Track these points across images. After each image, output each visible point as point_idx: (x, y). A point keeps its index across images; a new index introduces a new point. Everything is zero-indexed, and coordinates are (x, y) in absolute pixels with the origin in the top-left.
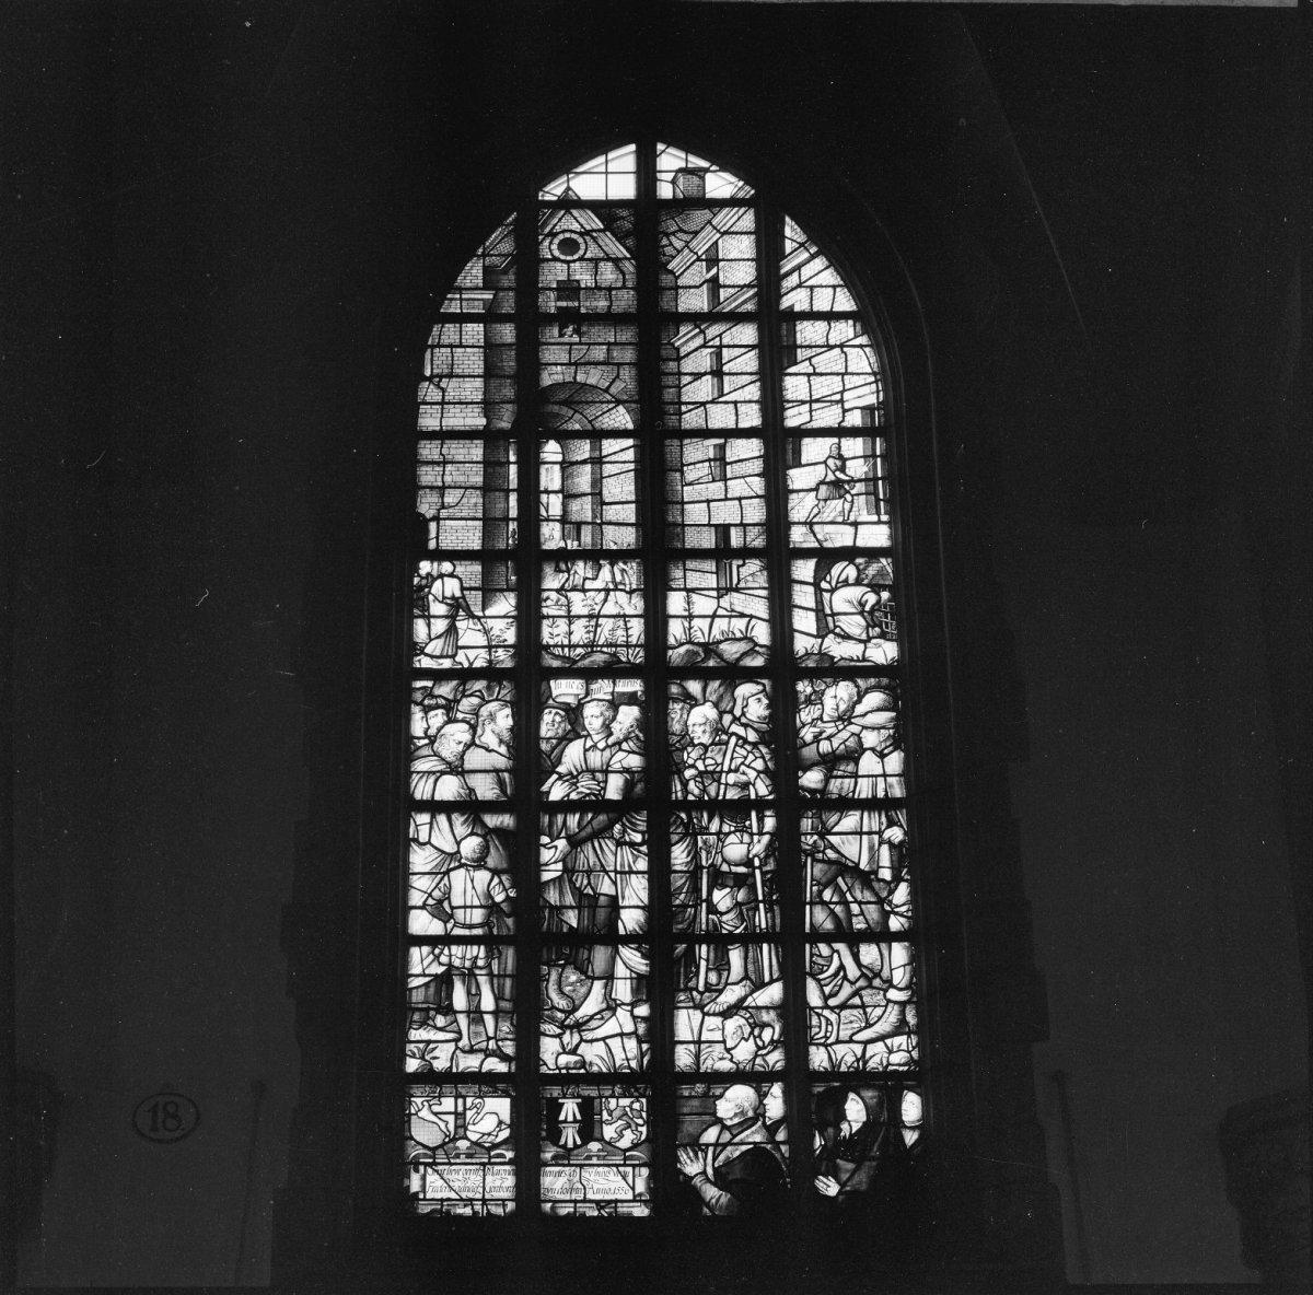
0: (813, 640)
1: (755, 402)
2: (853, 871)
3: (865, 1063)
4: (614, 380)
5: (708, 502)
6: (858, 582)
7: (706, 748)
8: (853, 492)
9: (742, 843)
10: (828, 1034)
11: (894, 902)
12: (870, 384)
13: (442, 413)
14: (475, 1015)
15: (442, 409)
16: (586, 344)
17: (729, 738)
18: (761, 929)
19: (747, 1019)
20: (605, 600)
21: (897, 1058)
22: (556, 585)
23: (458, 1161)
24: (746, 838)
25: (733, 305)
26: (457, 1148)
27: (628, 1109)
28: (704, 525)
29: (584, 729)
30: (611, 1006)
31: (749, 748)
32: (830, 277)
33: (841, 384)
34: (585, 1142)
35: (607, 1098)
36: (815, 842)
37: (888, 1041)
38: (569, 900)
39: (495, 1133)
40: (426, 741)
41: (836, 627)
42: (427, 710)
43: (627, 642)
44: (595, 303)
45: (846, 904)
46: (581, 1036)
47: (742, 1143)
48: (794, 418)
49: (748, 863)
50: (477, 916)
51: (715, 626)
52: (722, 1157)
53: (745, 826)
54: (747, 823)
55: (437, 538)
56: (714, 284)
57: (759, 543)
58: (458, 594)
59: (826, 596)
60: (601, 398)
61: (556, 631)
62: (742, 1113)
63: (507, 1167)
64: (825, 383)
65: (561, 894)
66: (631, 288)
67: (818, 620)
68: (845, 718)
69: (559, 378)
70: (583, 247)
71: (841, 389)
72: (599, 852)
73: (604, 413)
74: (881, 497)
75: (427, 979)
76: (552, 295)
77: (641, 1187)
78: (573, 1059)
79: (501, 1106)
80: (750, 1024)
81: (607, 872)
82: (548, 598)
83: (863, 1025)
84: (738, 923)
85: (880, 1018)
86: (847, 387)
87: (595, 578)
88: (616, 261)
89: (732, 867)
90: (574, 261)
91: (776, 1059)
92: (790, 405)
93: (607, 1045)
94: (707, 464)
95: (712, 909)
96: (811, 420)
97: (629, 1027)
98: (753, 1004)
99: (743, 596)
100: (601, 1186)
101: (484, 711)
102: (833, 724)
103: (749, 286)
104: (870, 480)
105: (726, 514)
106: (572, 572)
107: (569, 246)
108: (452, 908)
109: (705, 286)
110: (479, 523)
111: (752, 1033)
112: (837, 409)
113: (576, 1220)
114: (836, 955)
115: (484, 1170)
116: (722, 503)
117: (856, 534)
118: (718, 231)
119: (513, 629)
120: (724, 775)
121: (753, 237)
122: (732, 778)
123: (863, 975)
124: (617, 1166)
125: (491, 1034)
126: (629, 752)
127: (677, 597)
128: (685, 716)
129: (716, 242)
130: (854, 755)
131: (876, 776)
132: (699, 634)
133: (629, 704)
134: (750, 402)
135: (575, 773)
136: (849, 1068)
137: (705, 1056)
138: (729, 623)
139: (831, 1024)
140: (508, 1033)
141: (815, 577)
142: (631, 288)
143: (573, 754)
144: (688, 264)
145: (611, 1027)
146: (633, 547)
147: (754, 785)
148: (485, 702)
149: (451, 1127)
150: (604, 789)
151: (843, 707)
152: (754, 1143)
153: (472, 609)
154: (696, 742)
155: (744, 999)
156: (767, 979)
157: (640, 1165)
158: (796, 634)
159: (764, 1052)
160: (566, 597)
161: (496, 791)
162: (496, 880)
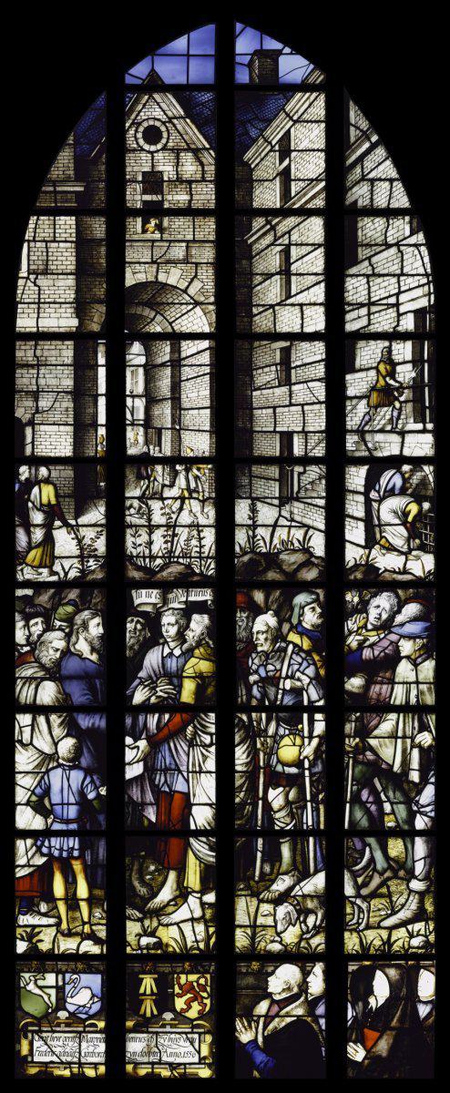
0: (361, 551)
1: (320, 304)
2: (386, 773)
3: (391, 945)
4: (192, 280)
5: (274, 408)
6: (403, 492)
7: (267, 654)
8: (402, 399)
9: (294, 745)
10: (360, 921)
11: (420, 802)
12: (423, 285)
13: (38, 313)
14: (72, 903)
15: (39, 308)
16: (166, 241)
17: (287, 646)
18: (308, 826)
19: (294, 906)
20: (181, 509)
21: (416, 942)
22: (137, 493)
23: (58, 1029)
24: (298, 741)
25: (303, 200)
26: (58, 1018)
27: (195, 984)
28: (270, 432)
29: (163, 636)
30: (183, 894)
31: (303, 655)
32: (388, 169)
33: (397, 286)
34: (161, 1012)
35: (178, 974)
36: (357, 744)
37: (410, 927)
38: (149, 797)
39: (89, 1005)
40: (28, 648)
41: (382, 537)
42: (27, 618)
43: (200, 552)
44: (177, 197)
45: (379, 803)
46: (159, 921)
47: (288, 1015)
48: (354, 322)
49: (299, 763)
50: (72, 812)
51: (277, 534)
52: (271, 1027)
53: (297, 729)
54: (300, 726)
55: (33, 442)
56: (285, 176)
57: (319, 452)
58: (53, 501)
59: (375, 505)
60: (180, 298)
61: (139, 541)
62: (289, 989)
63: (98, 1035)
64: (383, 285)
65: (143, 792)
66: (210, 181)
67: (367, 530)
68: (386, 626)
69: (141, 278)
70: (165, 135)
71: (397, 291)
72: (174, 751)
73: (183, 315)
74: (427, 404)
75: (31, 869)
76: (139, 187)
77: (205, 1051)
78: (152, 940)
79: (95, 981)
80: (296, 910)
81: (180, 772)
82: (131, 506)
83: (389, 912)
84: (288, 820)
85: (403, 906)
86: (402, 289)
87: (172, 485)
88: (196, 152)
89: (285, 768)
90: (157, 151)
91: (318, 941)
92: (351, 308)
93: (180, 928)
94: (273, 368)
95: (268, 807)
96: (369, 324)
97: (198, 914)
98: (300, 893)
99: (302, 506)
100: (172, 1051)
101: (78, 620)
102: (375, 633)
103: (317, 180)
104: (417, 386)
105: (289, 420)
106: (152, 479)
107: (152, 135)
108: (52, 805)
109: (278, 179)
110: (70, 429)
111: (298, 918)
112: (392, 313)
113: (153, 1078)
114: (368, 849)
115: (80, 1038)
116: (286, 409)
117: (403, 443)
118: (291, 118)
119: (103, 538)
120: (282, 680)
121: (323, 125)
122: (288, 684)
123: (390, 867)
124: (186, 1033)
125: (86, 919)
126: (200, 659)
127: (242, 505)
128: (250, 624)
129: (288, 132)
130: (394, 659)
131: (410, 683)
132: (262, 543)
133: (200, 612)
134: (315, 304)
135: (155, 679)
136: (376, 950)
137: (259, 939)
138: (289, 533)
139: (363, 912)
140: (100, 919)
141: (365, 486)
142: (210, 181)
143: (153, 659)
144: (263, 155)
145: (183, 913)
146: (207, 454)
147: (306, 691)
148: (78, 611)
149: (53, 999)
150: (180, 692)
151: (384, 616)
152: (298, 1016)
153: (67, 517)
154: (259, 649)
155: (291, 889)
156: (312, 870)
157: (205, 1033)
158: (348, 545)
159: (308, 936)
160: (147, 505)
161: (87, 697)
162: (88, 780)
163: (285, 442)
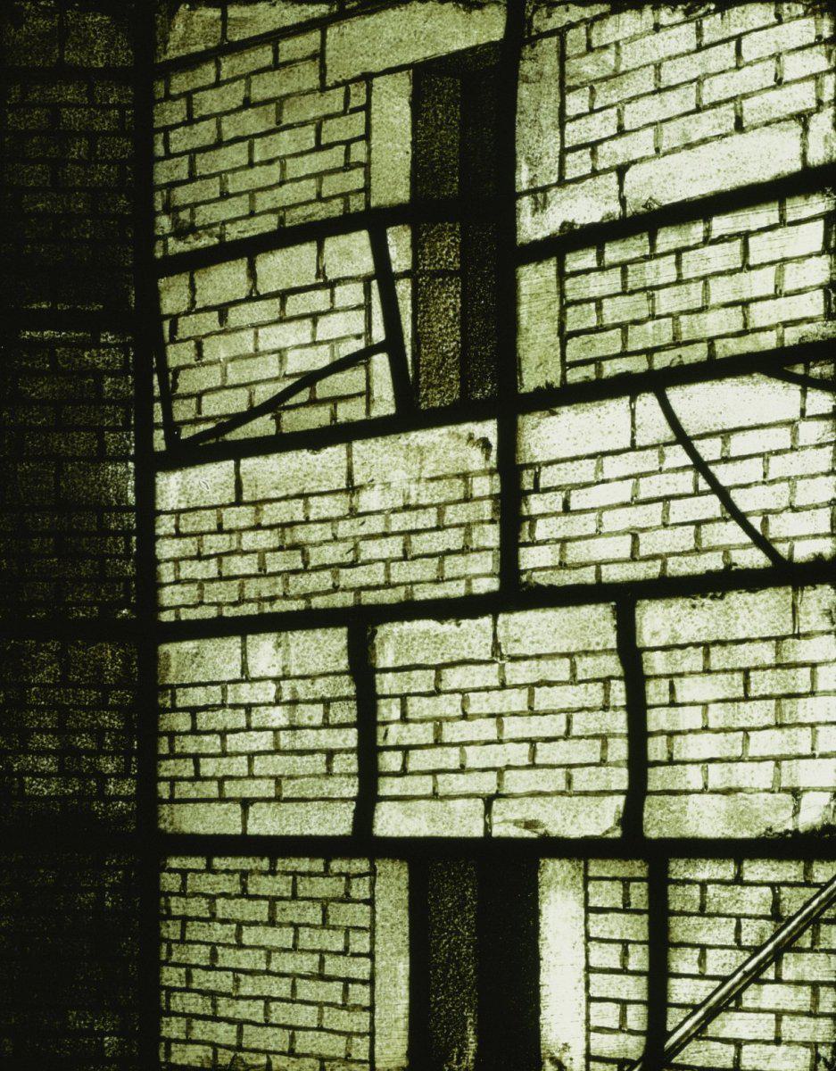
116: (473, 634)
163: (460, 934)
